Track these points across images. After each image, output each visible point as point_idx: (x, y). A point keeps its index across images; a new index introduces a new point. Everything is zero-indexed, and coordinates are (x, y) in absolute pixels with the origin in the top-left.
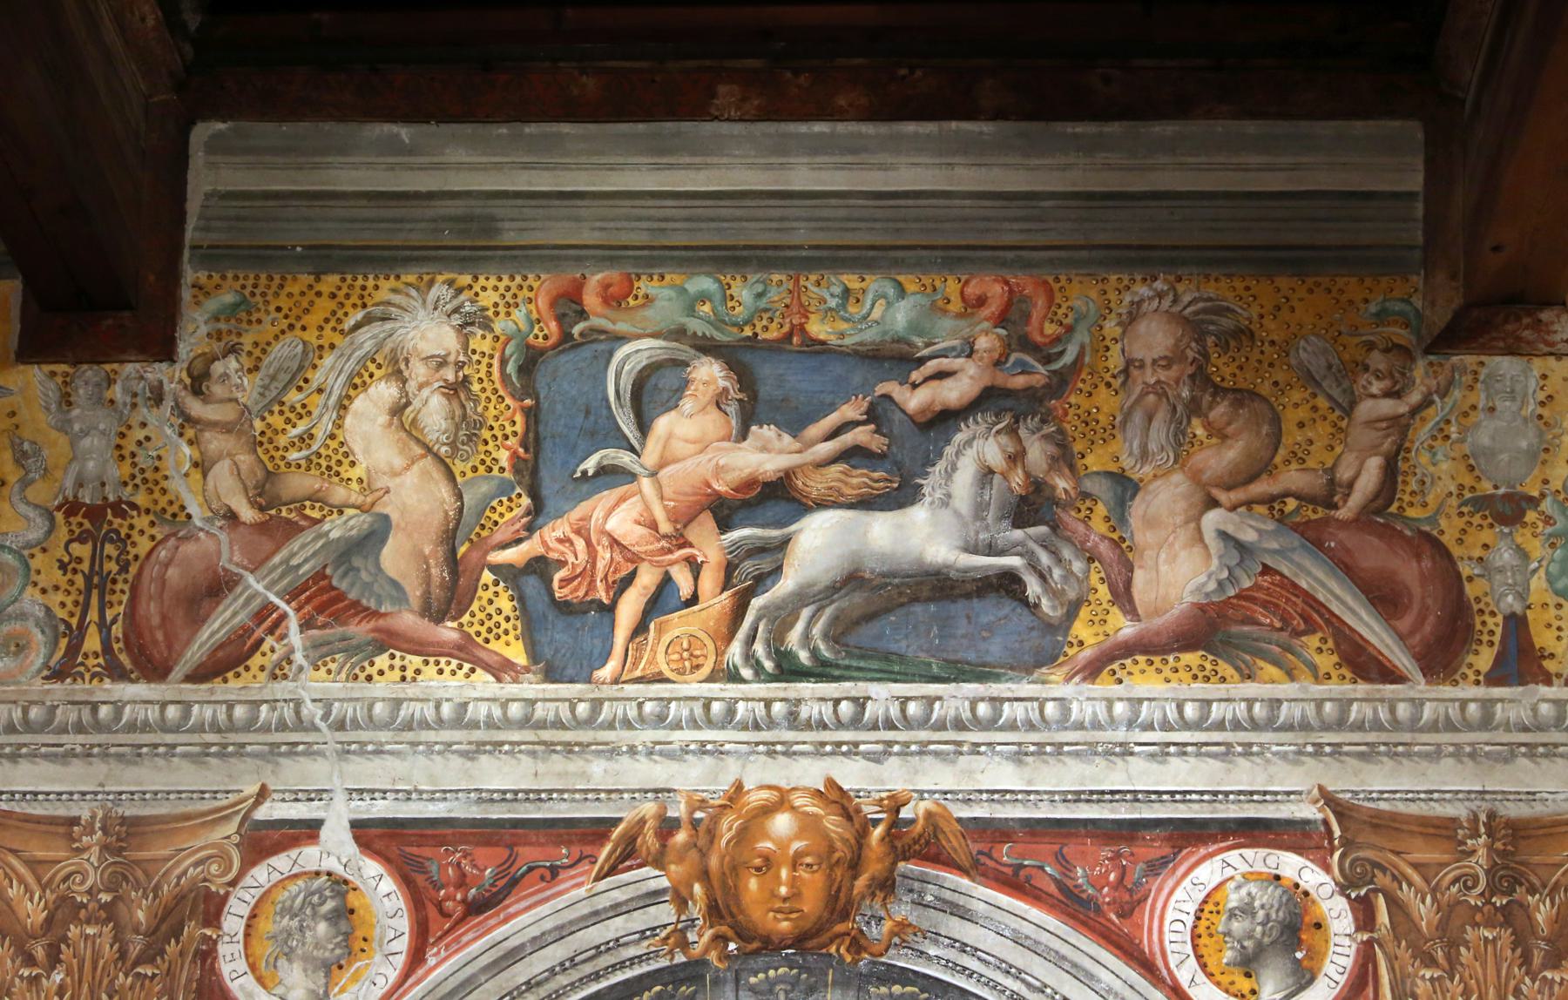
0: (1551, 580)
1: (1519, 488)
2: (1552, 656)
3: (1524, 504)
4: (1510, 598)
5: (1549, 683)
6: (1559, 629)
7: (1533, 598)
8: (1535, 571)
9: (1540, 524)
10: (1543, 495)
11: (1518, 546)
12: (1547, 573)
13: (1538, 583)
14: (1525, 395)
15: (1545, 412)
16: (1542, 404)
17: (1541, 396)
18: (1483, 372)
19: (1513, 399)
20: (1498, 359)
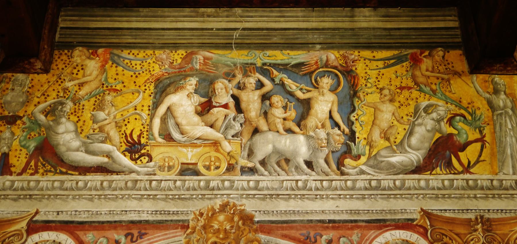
0: (20, 142)
1: (17, 114)
2: (14, 166)
3: (17, 118)
4: (5, 148)
5: (11, 174)
6: (19, 157)
7: (14, 148)
8: (15, 139)
9: (21, 125)
10: (24, 116)
11: (12, 132)
12: (20, 140)
13: (16, 143)
14: (25, 85)
15: (30, 90)
16: (30, 88)
17: (30, 85)
18: (13, 78)
19: (21, 86)
20: (19, 74)
